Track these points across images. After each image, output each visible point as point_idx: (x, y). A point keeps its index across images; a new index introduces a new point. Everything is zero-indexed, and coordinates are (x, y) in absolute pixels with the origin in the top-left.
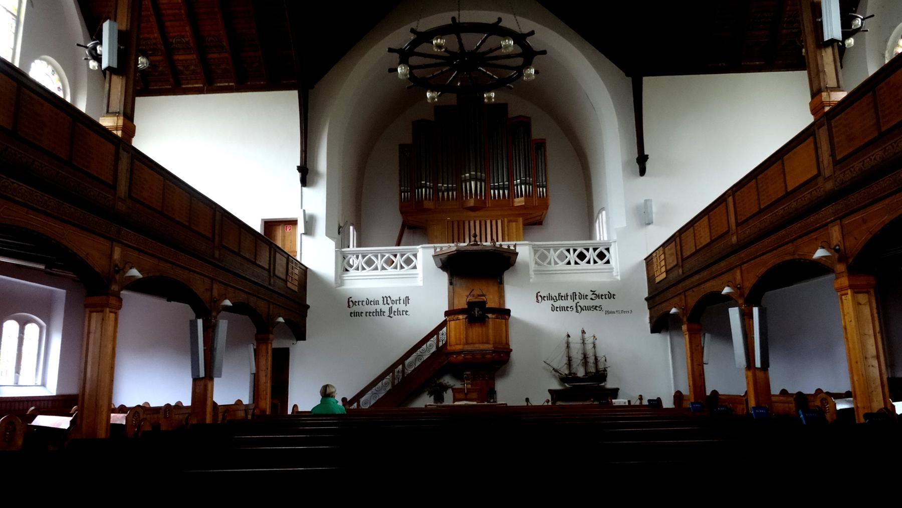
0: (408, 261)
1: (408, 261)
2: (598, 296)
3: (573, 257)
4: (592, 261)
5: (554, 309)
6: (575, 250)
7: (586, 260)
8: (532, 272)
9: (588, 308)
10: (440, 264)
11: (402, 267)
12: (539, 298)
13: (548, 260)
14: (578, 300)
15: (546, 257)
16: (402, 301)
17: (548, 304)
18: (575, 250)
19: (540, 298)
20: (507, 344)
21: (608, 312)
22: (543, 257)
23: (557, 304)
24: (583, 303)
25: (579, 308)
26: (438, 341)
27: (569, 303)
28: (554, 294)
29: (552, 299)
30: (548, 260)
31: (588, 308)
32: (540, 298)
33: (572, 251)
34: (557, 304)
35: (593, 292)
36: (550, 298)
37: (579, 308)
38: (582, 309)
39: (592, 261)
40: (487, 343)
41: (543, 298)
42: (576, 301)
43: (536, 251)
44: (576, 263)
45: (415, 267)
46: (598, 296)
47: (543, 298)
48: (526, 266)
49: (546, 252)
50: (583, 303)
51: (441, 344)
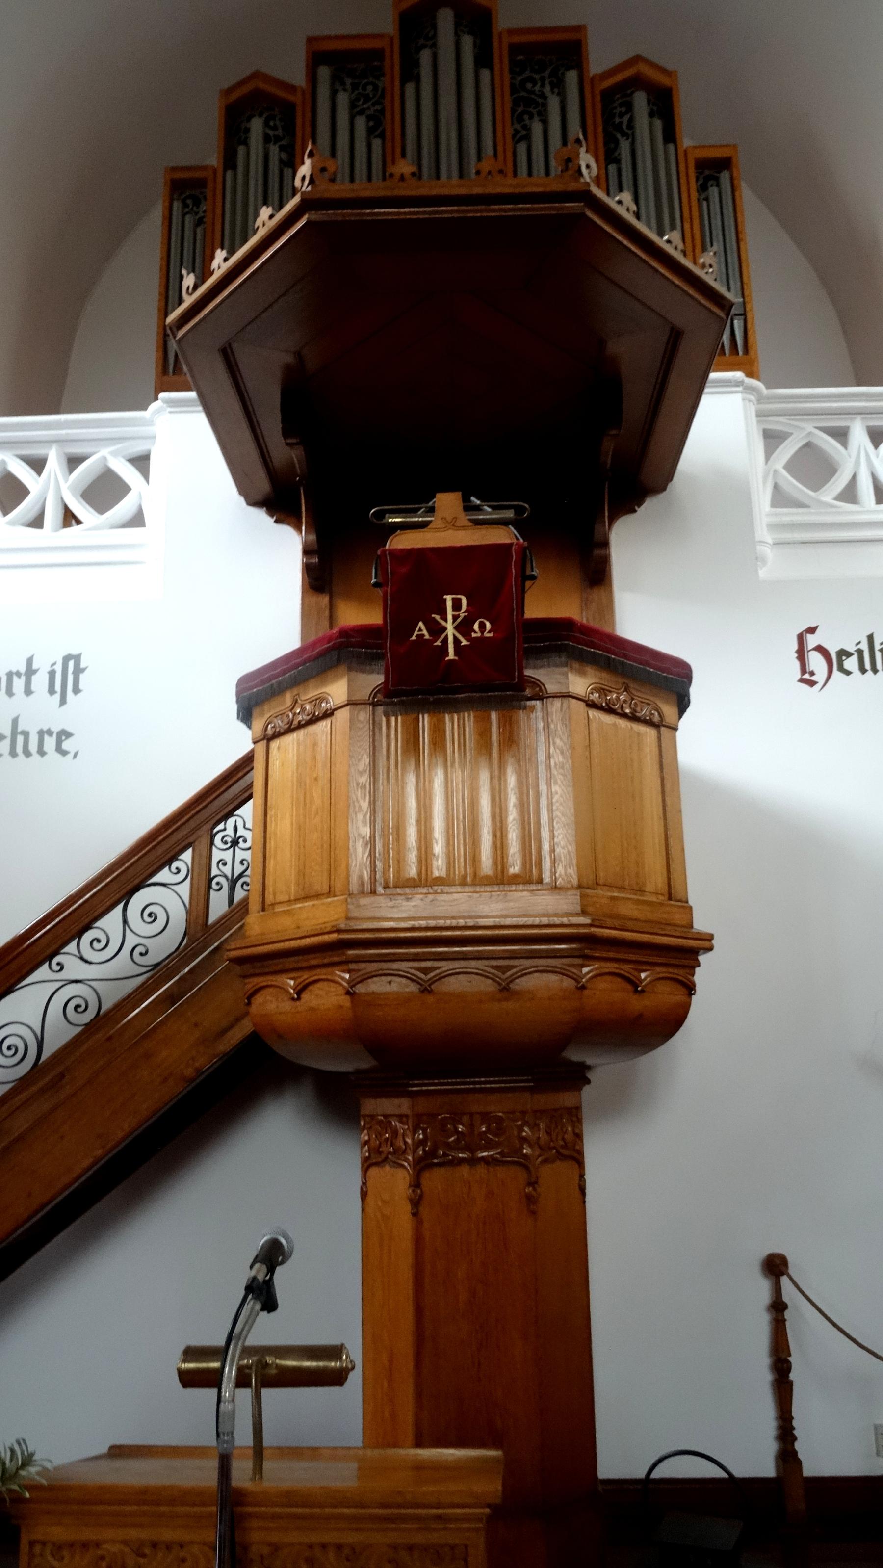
0: (105, 491)
1: (105, 491)
8: (763, 533)
10: (264, 486)
11: (69, 518)
13: (840, 482)
15: (829, 469)
16: (40, 681)
19: (816, 662)
20: (674, 895)
22: (814, 467)
26: (203, 883)
30: (840, 482)
32: (816, 662)
40: (529, 878)
43: (772, 439)
45: (137, 520)
47: (836, 661)
48: (733, 491)
49: (829, 444)
51: (218, 905)
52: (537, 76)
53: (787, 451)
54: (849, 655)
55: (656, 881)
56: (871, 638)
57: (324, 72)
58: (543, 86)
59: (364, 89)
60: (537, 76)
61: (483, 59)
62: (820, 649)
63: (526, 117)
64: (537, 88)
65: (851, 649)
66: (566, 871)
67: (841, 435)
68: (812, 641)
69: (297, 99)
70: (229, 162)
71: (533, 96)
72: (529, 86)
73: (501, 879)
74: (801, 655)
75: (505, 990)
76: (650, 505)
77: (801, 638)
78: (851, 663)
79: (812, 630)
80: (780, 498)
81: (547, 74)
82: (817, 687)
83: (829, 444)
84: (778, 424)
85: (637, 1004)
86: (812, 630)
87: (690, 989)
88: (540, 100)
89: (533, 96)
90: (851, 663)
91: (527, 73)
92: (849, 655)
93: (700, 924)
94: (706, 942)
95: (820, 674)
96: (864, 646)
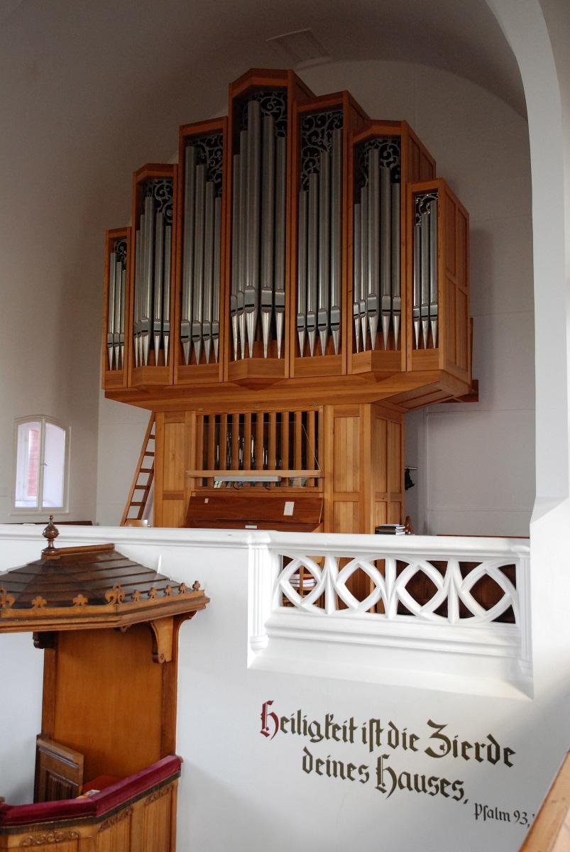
5: (310, 764)
14: (385, 748)
17: (292, 744)
23: (323, 750)
25: (387, 778)
27: (355, 752)
28: (314, 715)
29: (308, 731)
31: (417, 784)
32: (270, 722)
34: (323, 750)
35: (437, 730)
37: (387, 778)
38: (396, 782)
41: (280, 723)
42: (379, 751)
46: (451, 746)
50: (402, 761)
52: (319, 130)
54: (287, 721)
56: (299, 713)
57: (190, 150)
58: (322, 138)
59: (216, 155)
60: (319, 130)
61: (281, 126)
62: (273, 715)
63: (311, 164)
64: (319, 139)
65: (289, 717)
68: (270, 709)
69: (174, 174)
70: (138, 227)
71: (315, 147)
72: (314, 138)
77: (264, 706)
79: (270, 703)
81: (325, 127)
82: (269, 737)
86: (270, 703)
88: (320, 149)
89: (315, 147)
90: (288, 726)
91: (313, 129)
92: (287, 721)
95: (271, 732)
96: (296, 717)
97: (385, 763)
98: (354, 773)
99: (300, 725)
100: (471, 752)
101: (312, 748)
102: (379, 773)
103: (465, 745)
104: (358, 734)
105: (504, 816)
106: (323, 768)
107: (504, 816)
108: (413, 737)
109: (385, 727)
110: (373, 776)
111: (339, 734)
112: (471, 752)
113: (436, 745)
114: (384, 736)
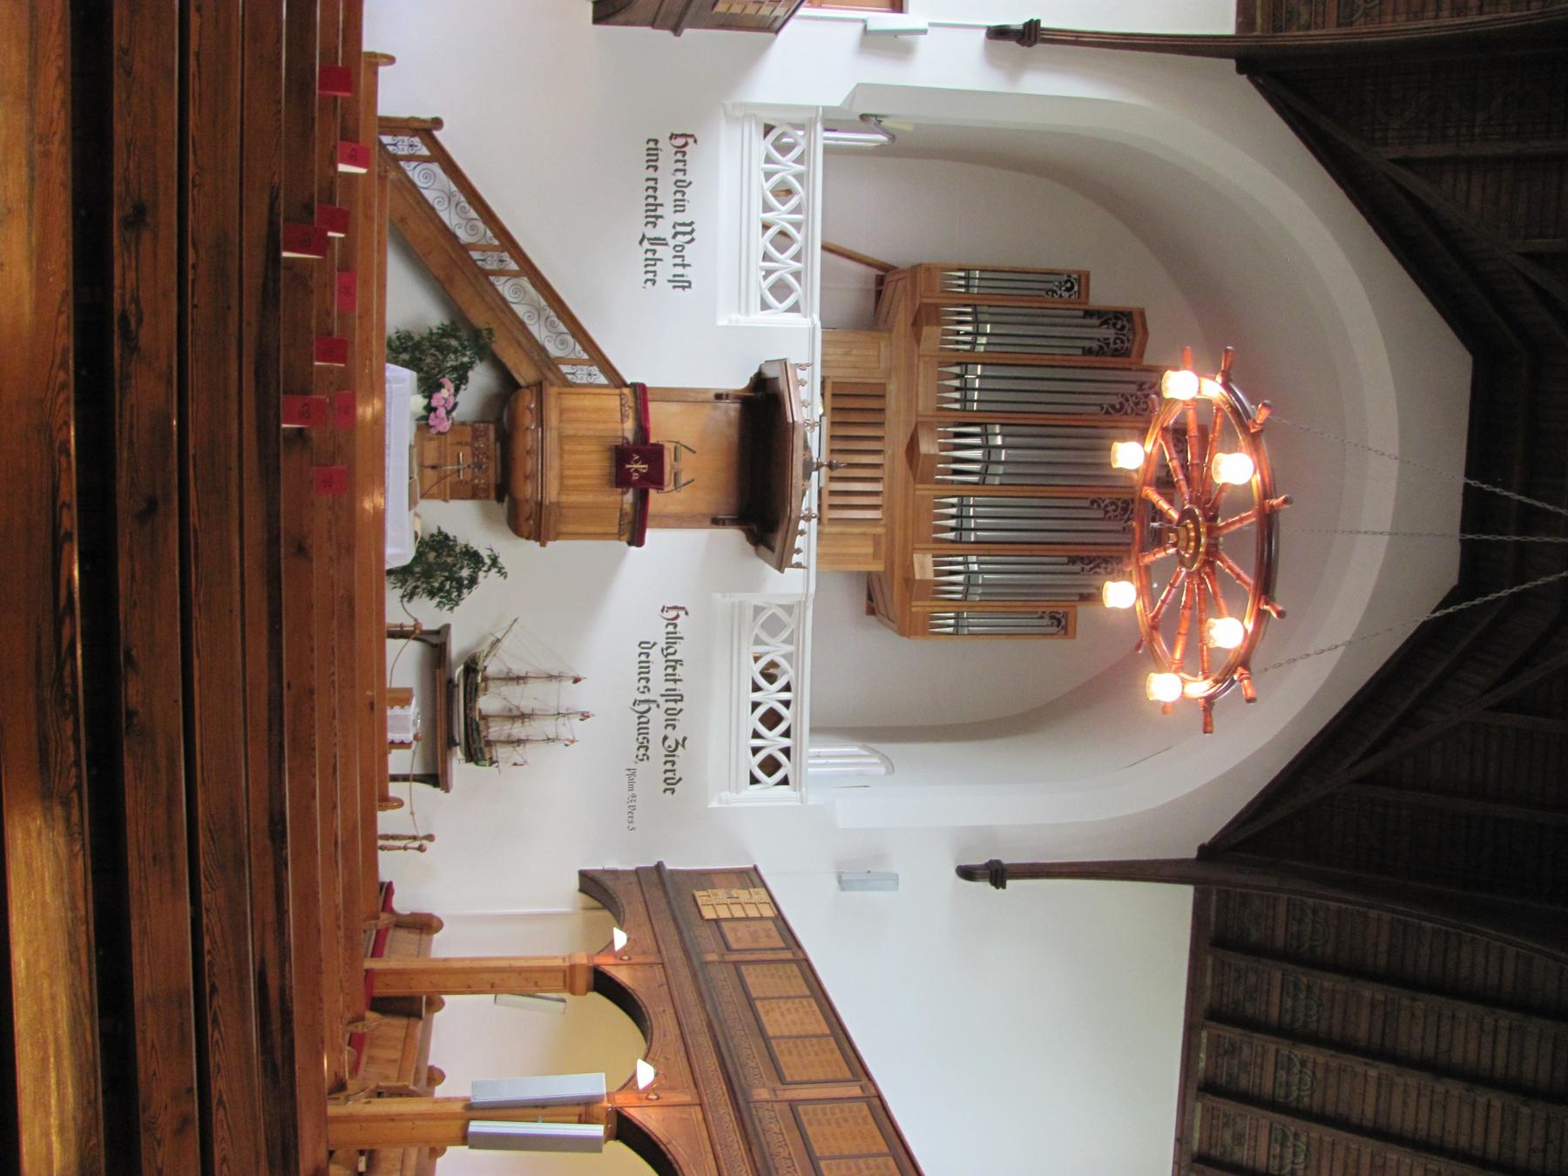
2: (672, 753)
3: (771, 696)
4: (758, 742)
5: (645, 646)
6: (787, 704)
7: (762, 729)
8: (737, 597)
9: (643, 728)
12: (674, 614)
13: (764, 636)
14: (664, 706)
15: (773, 635)
17: (659, 635)
18: (787, 704)
19: (673, 614)
21: (632, 773)
23: (656, 654)
24: (657, 717)
25: (644, 707)
27: (658, 685)
28: (681, 650)
30: (764, 636)
32: (673, 614)
33: (785, 696)
34: (656, 654)
36: (673, 639)
37: (644, 707)
39: (758, 742)
41: (672, 622)
42: (661, 700)
43: (789, 609)
44: (755, 705)
46: (672, 753)
47: (672, 622)
49: (785, 634)
50: (657, 717)
53: (781, 614)
55: (564, 529)
66: (564, 498)
67: (788, 641)
68: (682, 613)
73: (562, 477)
74: (675, 608)
75: (527, 477)
76: (751, 548)
78: (671, 629)
80: (758, 610)
83: (785, 634)
84: (796, 610)
85: (522, 519)
87: (528, 538)
90: (671, 629)
93: (550, 544)
94: (543, 545)
95: (665, 615)
97: (653, 706)
98: (643, 682)
99: (673, 639)
100: (669, 766)
101: (657, 649)
102: (647, 701)
103: (674, 763)
104: (671, 685)
105: (631, 788)
106: (643, 658)
107: (631, 788)
108: (674, 727)
109: (679, 706)
110: (643, 697)
111: (670, 671)
112: (669, 766)
113: (671, 742)
114: (672, 705)
